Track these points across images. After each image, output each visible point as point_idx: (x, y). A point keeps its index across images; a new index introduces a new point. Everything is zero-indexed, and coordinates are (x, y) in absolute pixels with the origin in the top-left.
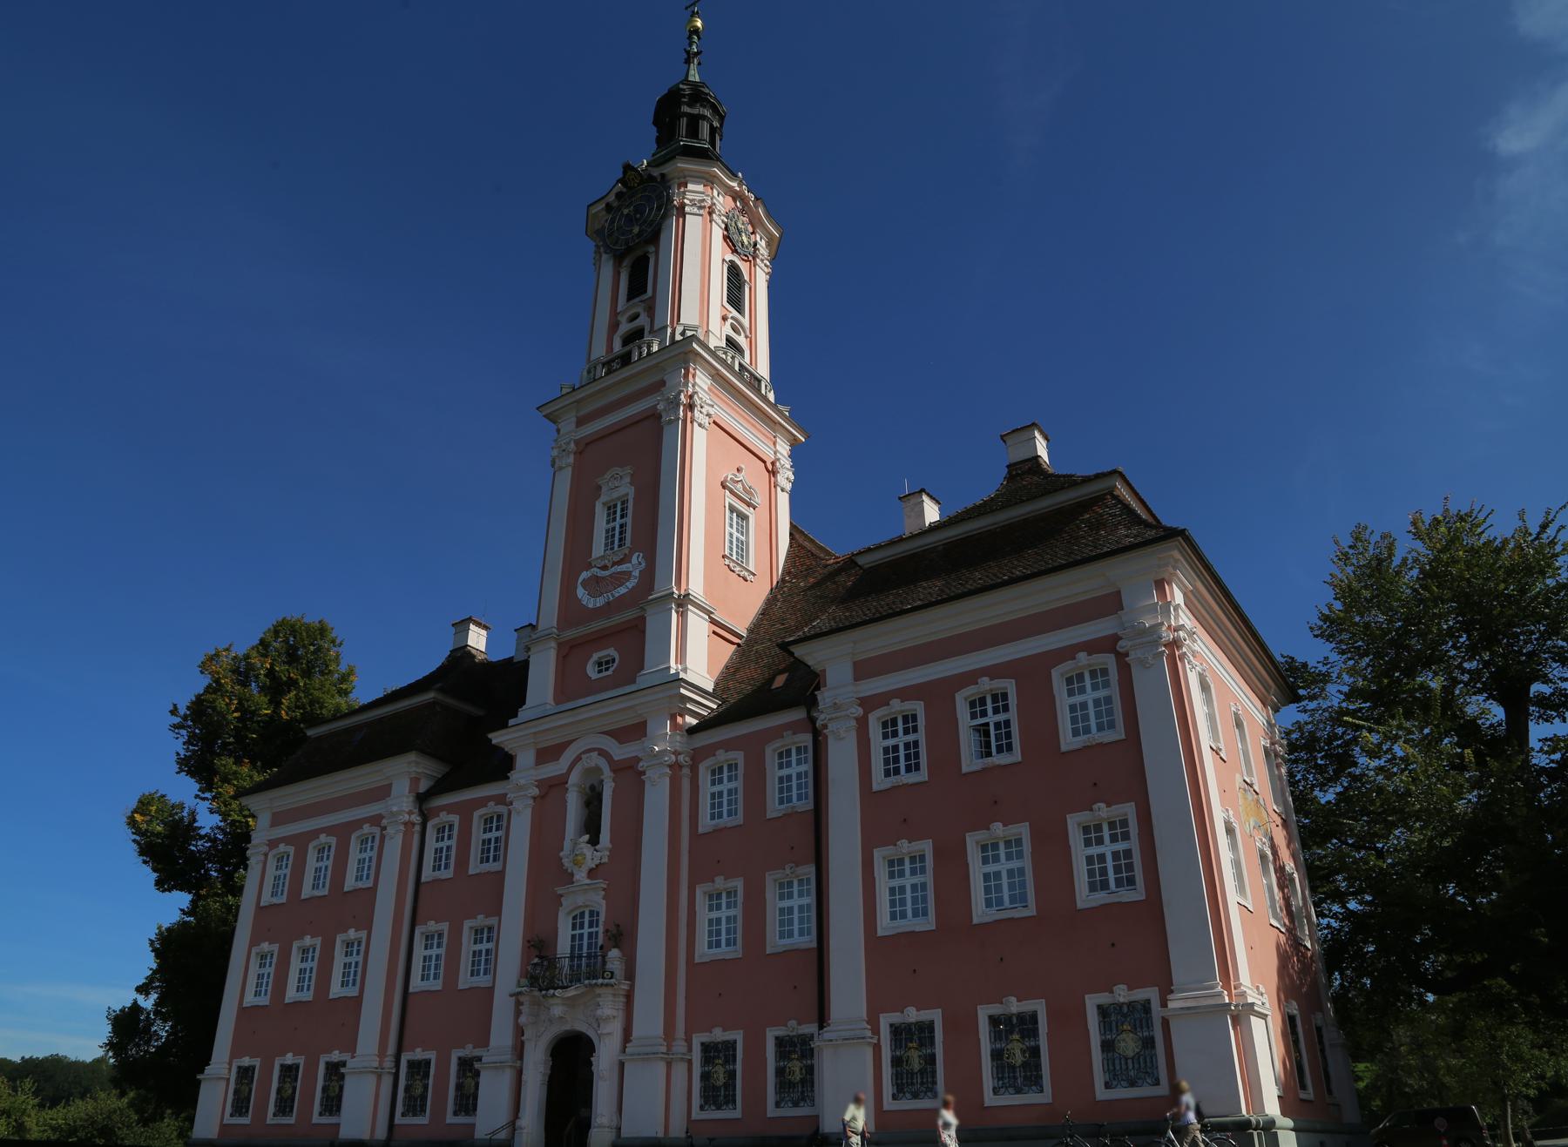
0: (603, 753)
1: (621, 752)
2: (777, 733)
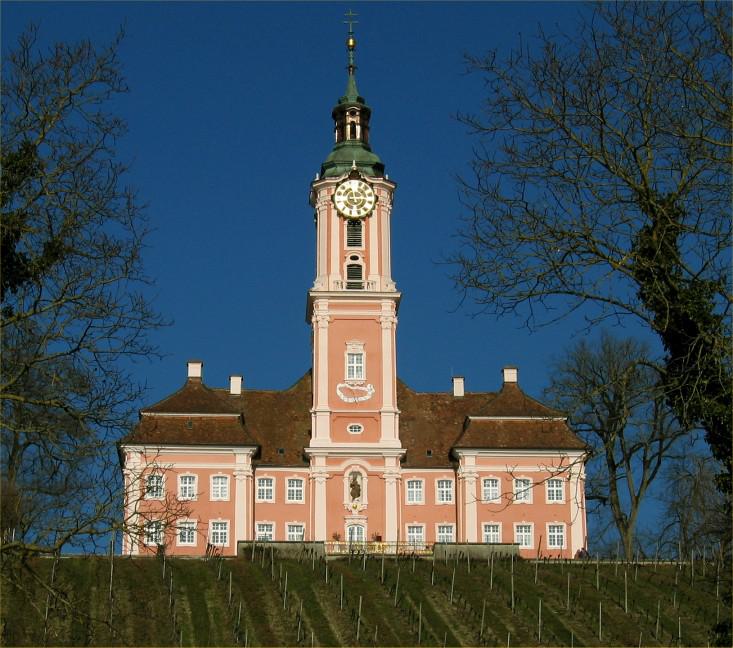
0: (361, 467)
1: (371, 468)
2: (441, 475)
